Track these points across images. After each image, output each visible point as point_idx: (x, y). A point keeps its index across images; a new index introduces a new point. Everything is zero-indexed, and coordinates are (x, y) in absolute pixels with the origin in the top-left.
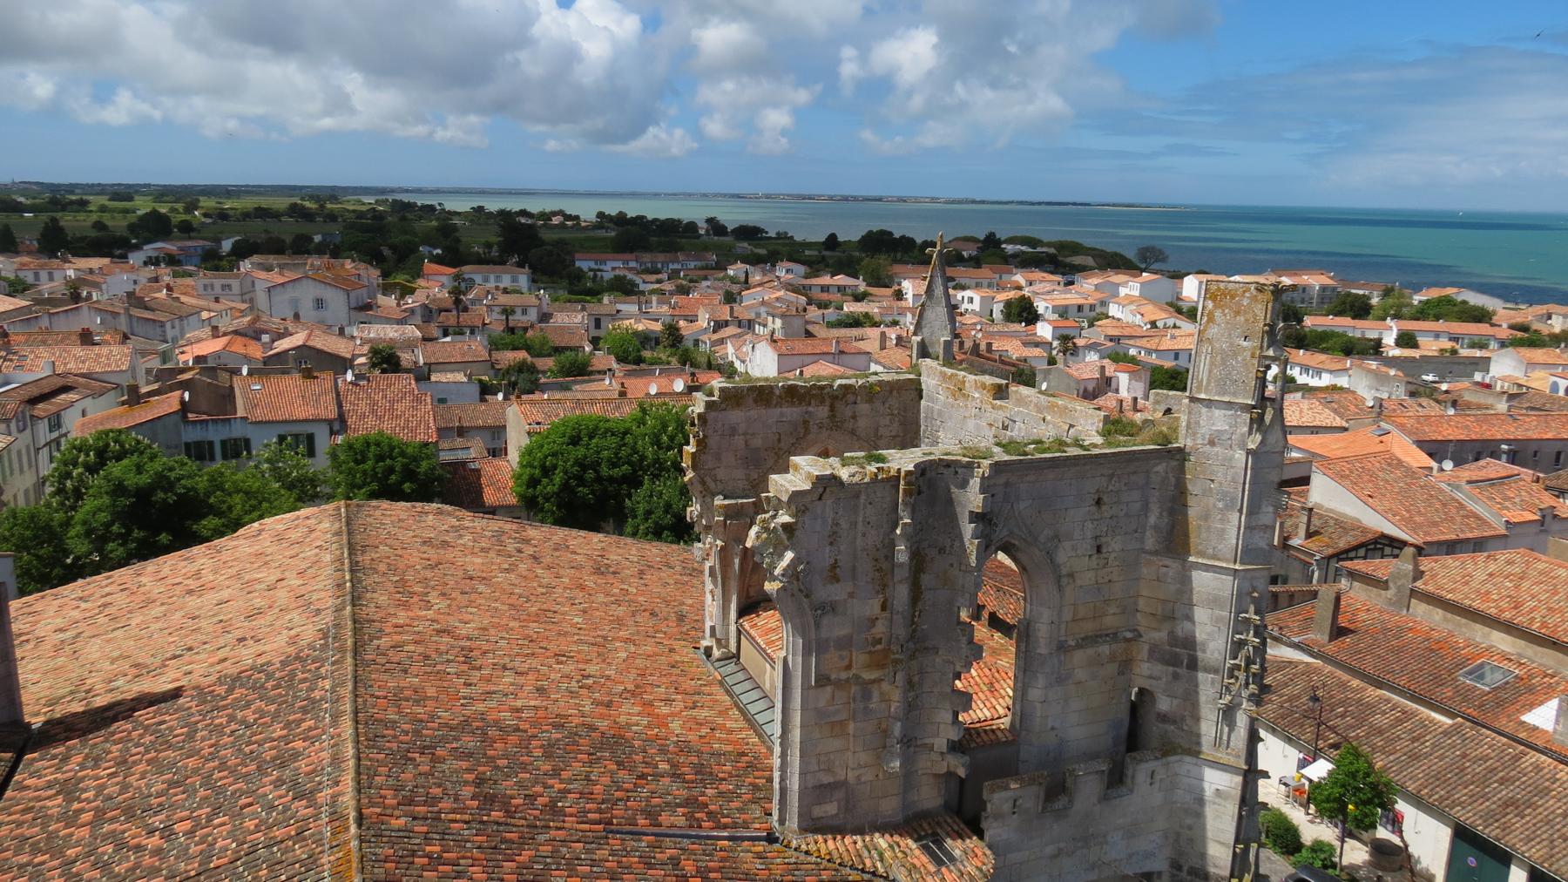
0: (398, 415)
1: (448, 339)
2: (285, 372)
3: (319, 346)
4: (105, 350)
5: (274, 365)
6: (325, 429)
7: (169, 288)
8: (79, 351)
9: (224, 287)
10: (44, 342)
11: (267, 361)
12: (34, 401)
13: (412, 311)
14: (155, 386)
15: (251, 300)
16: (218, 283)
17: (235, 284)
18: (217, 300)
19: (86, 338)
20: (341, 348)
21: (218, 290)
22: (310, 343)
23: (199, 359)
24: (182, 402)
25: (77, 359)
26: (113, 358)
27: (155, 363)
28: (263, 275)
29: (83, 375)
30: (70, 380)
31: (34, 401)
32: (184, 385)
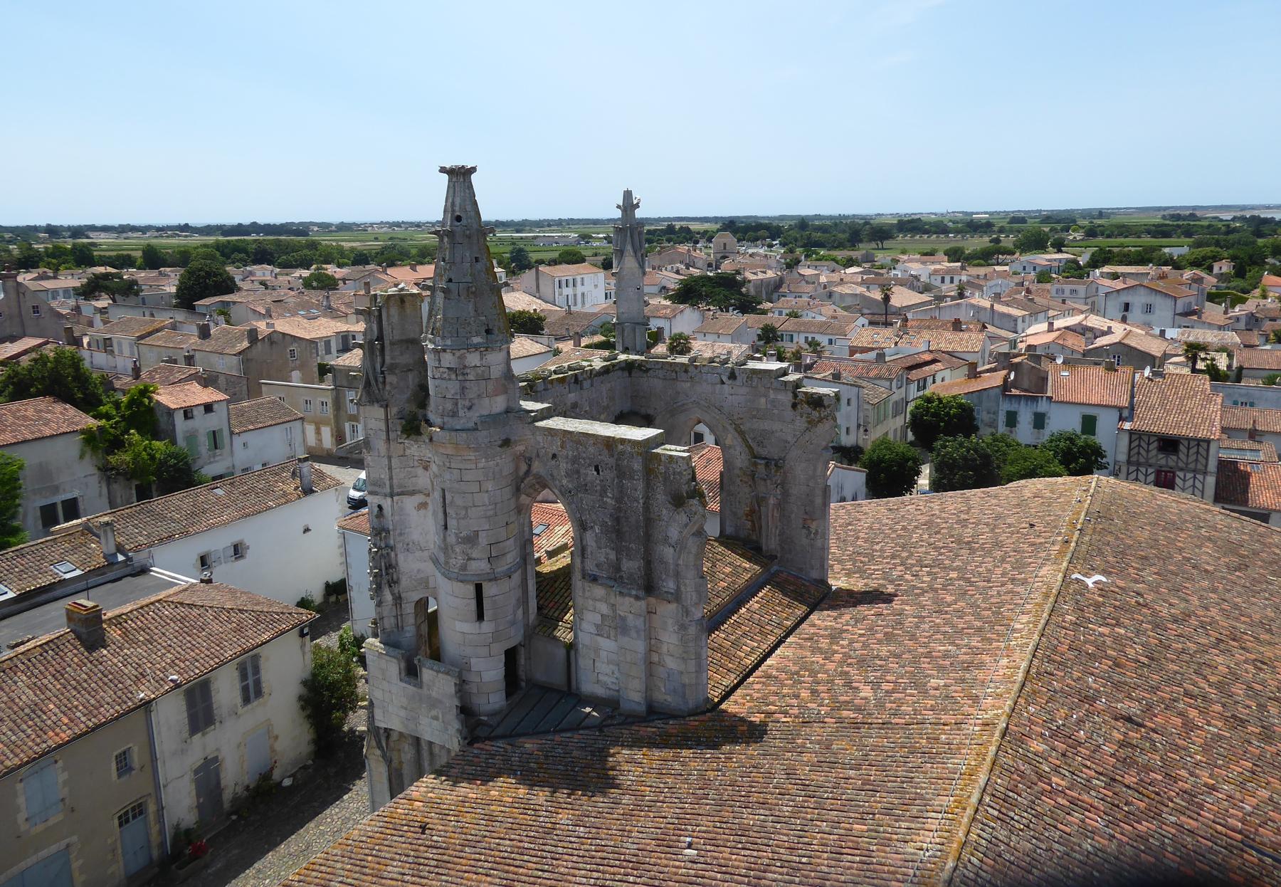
0: (1197, 412)
1: (1268, 347)
2: (1096, 364)
3: (1133, 344)
4: (966, 335)
5: (1092, 357)
6: (1116, 414)
7: (1028, 291)
8: (949, 335)
9: (1073, 291)
10: (929, 327)
11: (1086, 354)
12: (911, 368)
13: (1238, 319)
14: (993, 366)
15: (1093, 303)
16: (1067, 288)
17: (1081, 289)
18: (1064, 302)
19: (957, 325)
20: (1155, 348)
21: (1067, 293)
22: (1126, 341)
23: (1030, 347)
24: (1006, 379)
25: (947, 341)
26: (970, 342)
27: (1005, 349)
28: (1107, 282)
29: (948, 353)
30: (938, 356)
31: (911, 368)
32: (1016, 367)
